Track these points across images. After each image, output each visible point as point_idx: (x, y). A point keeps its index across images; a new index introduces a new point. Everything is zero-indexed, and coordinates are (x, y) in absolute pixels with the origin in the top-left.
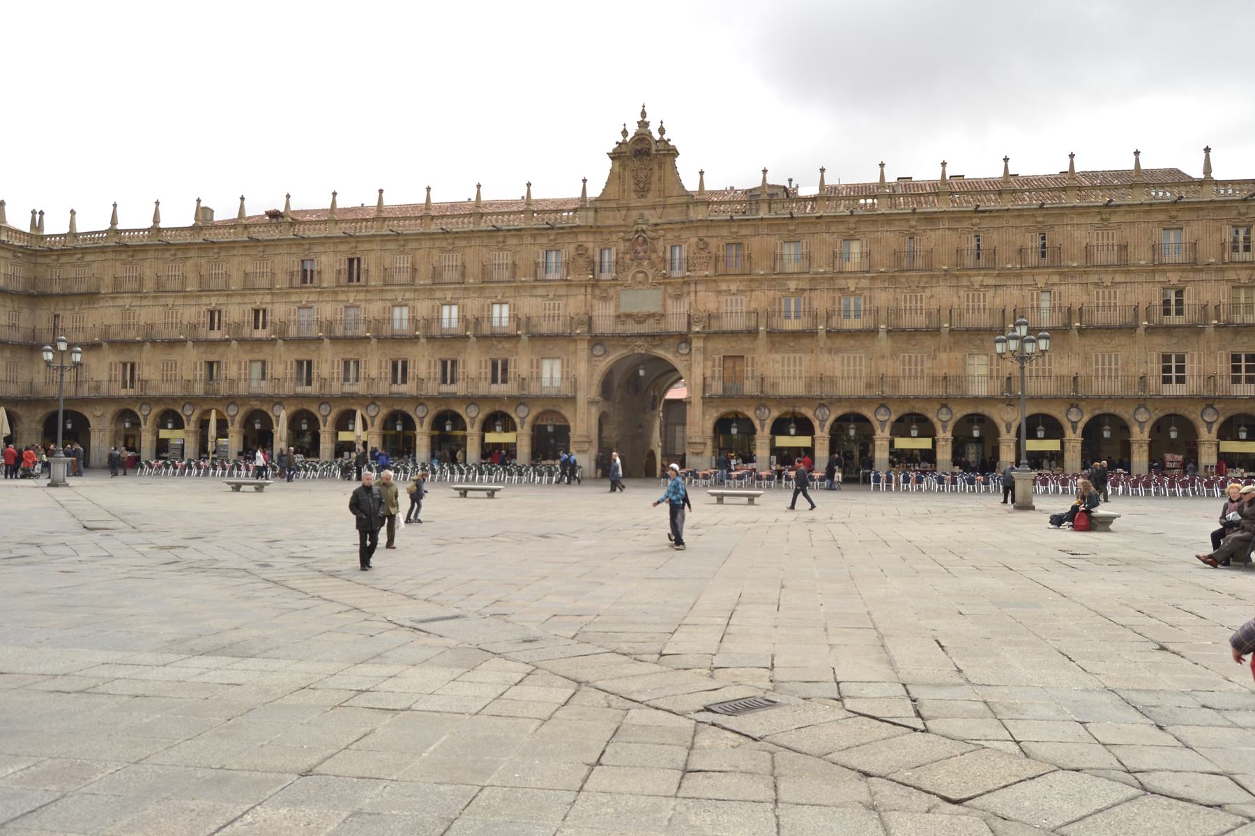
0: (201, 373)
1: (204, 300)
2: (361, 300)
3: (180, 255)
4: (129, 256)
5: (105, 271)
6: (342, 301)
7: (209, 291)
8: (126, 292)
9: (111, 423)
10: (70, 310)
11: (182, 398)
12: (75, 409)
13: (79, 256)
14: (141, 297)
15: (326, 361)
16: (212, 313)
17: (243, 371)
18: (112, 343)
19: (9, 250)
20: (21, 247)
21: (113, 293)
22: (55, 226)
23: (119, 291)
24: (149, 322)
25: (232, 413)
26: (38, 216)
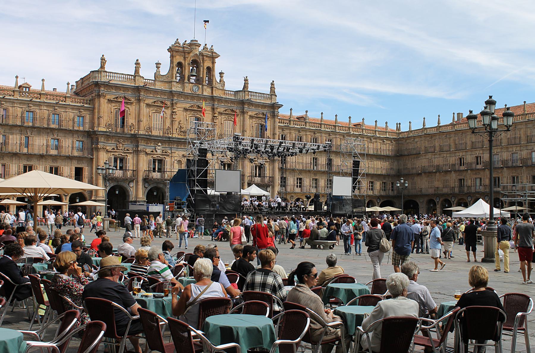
0: (457, 184)
1: (457, 154)
2: (518, 150)
4: (430, 138)
5: (422, 144)
6: (511, 151)
7: (459, 150)
8: (429, 153)
9: (426, 205)
11: (451, 194)
12: (413, 199)
15: (505, 177)
16: (461, 159)
17: (473, 183)
18: (425, 173)
19: (389, 140)
20: (393, 138)
21: (425, 153)
22: (404, 128)
23: (427, 152)
24: (438, 164)
25: (469, 200)
26: (398, 125)
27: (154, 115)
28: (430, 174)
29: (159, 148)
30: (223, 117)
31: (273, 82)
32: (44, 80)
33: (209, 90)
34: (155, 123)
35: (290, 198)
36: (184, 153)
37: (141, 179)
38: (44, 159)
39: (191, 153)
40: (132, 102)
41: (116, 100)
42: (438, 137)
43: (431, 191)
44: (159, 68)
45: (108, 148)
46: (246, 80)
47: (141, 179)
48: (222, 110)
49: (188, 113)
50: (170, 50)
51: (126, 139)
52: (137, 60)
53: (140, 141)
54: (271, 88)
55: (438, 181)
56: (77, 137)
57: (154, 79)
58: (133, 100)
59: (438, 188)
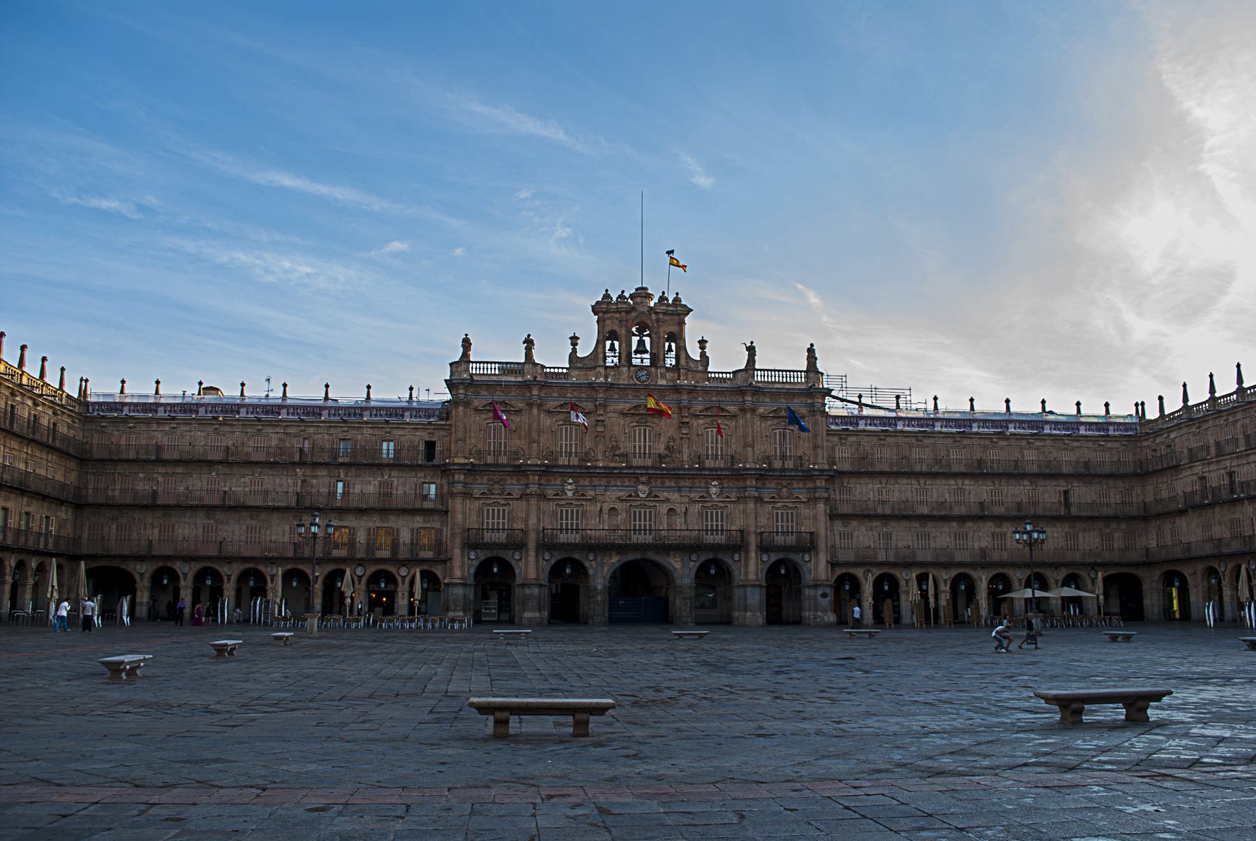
3: (1231, 419)
8: (1198, 461)
10: (1165, 482)
13: (1165, 436)
14: (1208, 463)
18: (1194, 508)
19: (1116, 441)
21: (1189, 463)
22: (1152, 413)
26: (1140, 407)
27: (562, 429)
28: (1202, 507)
29: (569, 487)
30: (701, 421)
31: (812, 345)
34: (564, 442)
35: (864, 574)
37: (532, 545)
39: (633, 494)
40: (517, 409)
42: (1210, 424)
43: (1208, 549)
44: (577, 344)
47: (532, 545)
49: (628, 419)
50: (595, 310)
51: (508, 476)
52: (529, 335)
53: (531, 477)
55: (1220, 524)
57: (568, 366)
58: (521, 405)
59: (1220, 540)
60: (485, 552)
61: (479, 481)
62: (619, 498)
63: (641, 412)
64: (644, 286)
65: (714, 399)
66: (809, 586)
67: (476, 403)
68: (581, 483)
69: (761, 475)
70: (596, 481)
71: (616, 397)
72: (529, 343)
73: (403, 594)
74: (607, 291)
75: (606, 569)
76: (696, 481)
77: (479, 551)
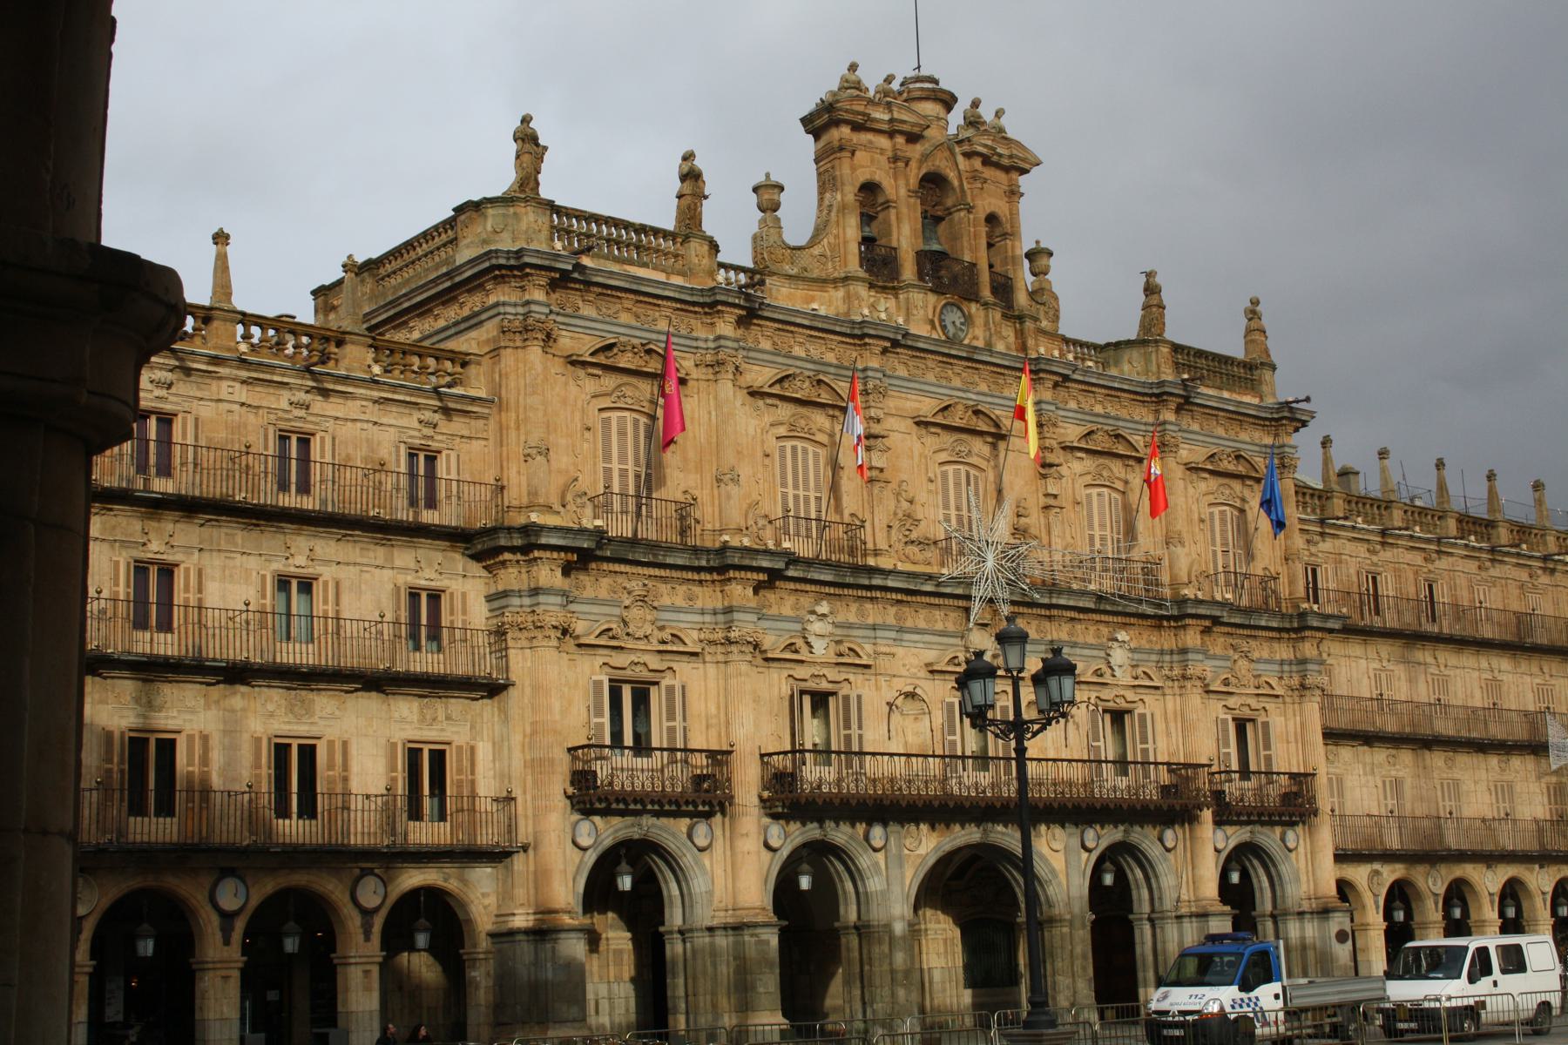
29: (817, 627)
30: (1077, 466)
31: (1255, 302)
32: (227, 237)
33: (1009, 332)
36: (930, 655)
38: (243, 695)
41: (601, 359)
44: (775, 207)
45: (580, 627)
46: (1151, 289)
48: (1072, 432)
49: (931, 441)
50: (819, 122)
54: (1249, 331)
56: (412, 565)
60: (616, 821)
61: (589, 593)
62: (927, 665)
63: (957, 423)
64: (924, 72)
65: (1098, 409)
66: (1301, 914)
67: (567, 342)
68: (840, 618)
69: (1216, 621)
70: (873, 613)
71: (902, 371)
72: (691, 176)
73: (367, 973)
74: (853, 67)
75: (909, 873)
76: (1079, 627)
77: (597, 819)
